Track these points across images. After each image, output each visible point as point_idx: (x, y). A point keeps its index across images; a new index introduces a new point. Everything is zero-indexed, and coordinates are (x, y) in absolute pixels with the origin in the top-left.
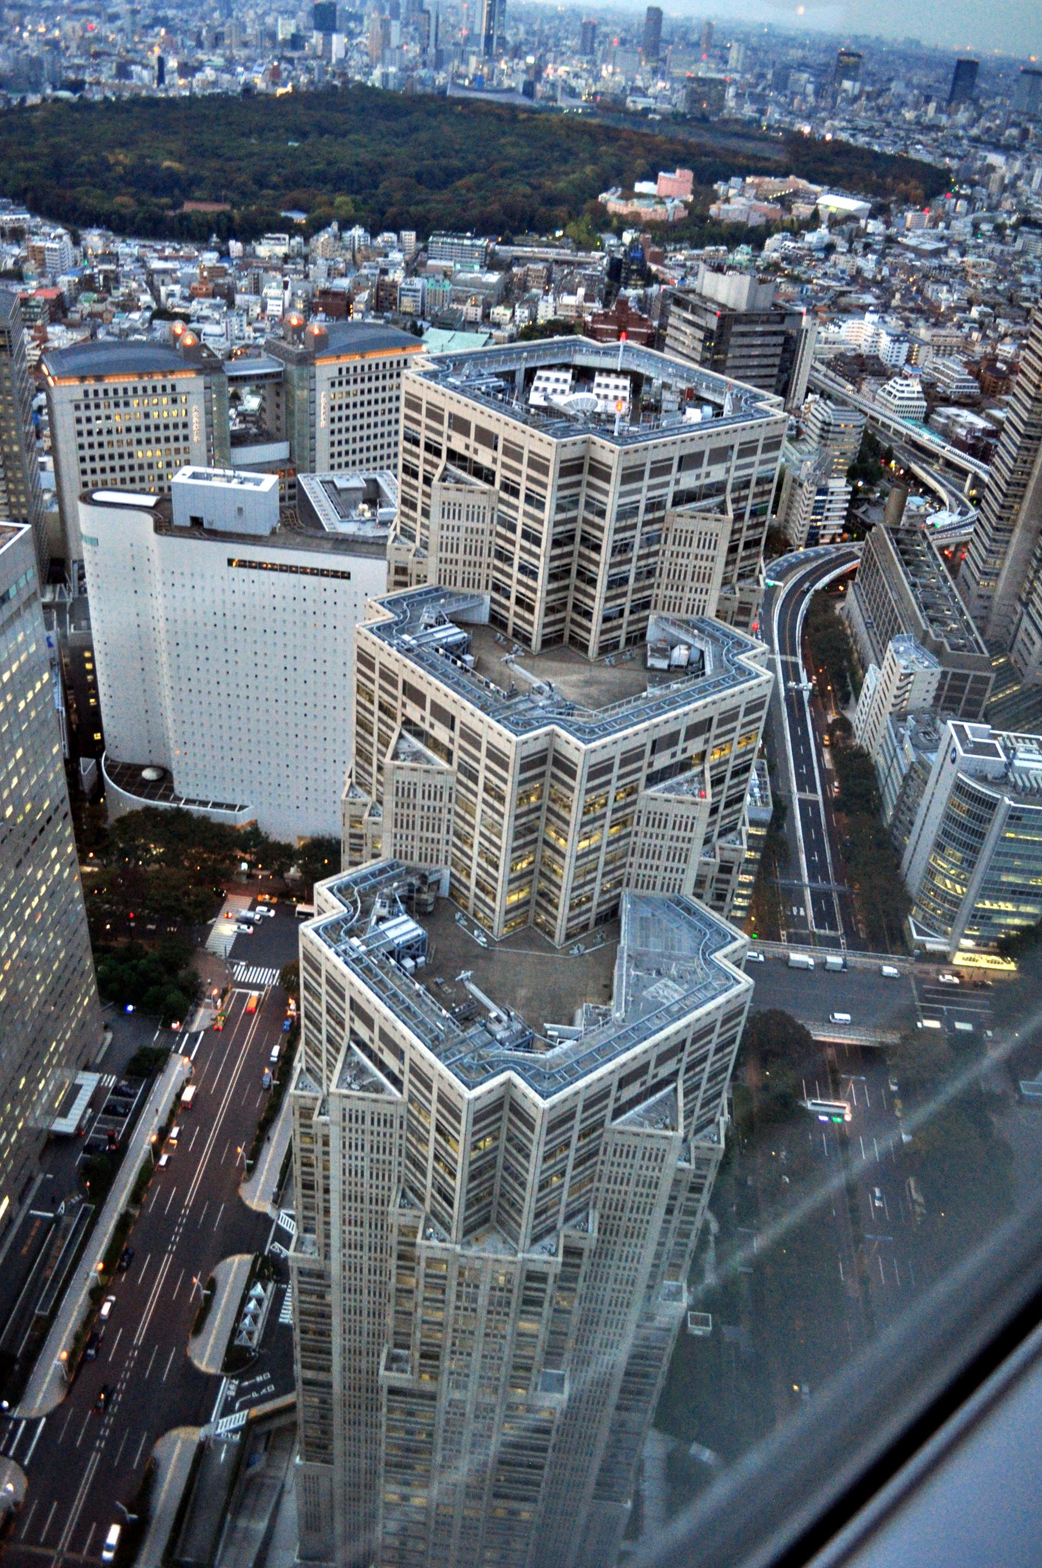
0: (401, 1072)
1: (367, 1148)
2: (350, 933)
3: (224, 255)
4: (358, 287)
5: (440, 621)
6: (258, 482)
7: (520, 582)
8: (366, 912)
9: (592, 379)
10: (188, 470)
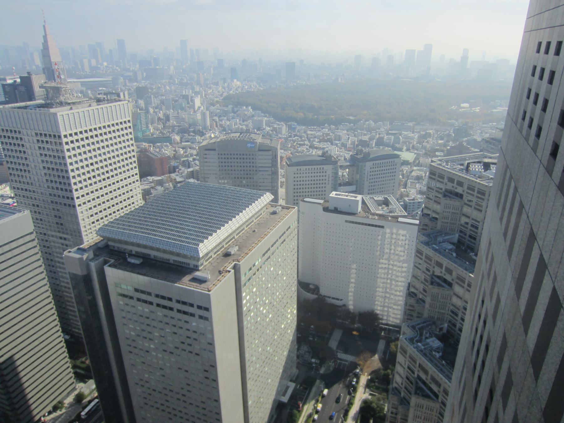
0: (439, 392)
1: (422, 418)
2: (417, 342)
3: (330, 129)
4: (371, 139)
5: (444, 241)
6: (356, 197)
7: (471, 230)
8: (421, 335)
9: (490, 166)
10: (334, 193)
